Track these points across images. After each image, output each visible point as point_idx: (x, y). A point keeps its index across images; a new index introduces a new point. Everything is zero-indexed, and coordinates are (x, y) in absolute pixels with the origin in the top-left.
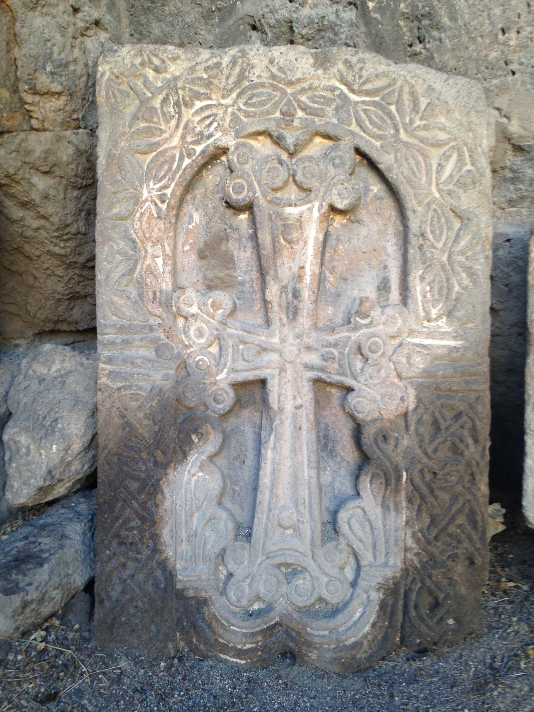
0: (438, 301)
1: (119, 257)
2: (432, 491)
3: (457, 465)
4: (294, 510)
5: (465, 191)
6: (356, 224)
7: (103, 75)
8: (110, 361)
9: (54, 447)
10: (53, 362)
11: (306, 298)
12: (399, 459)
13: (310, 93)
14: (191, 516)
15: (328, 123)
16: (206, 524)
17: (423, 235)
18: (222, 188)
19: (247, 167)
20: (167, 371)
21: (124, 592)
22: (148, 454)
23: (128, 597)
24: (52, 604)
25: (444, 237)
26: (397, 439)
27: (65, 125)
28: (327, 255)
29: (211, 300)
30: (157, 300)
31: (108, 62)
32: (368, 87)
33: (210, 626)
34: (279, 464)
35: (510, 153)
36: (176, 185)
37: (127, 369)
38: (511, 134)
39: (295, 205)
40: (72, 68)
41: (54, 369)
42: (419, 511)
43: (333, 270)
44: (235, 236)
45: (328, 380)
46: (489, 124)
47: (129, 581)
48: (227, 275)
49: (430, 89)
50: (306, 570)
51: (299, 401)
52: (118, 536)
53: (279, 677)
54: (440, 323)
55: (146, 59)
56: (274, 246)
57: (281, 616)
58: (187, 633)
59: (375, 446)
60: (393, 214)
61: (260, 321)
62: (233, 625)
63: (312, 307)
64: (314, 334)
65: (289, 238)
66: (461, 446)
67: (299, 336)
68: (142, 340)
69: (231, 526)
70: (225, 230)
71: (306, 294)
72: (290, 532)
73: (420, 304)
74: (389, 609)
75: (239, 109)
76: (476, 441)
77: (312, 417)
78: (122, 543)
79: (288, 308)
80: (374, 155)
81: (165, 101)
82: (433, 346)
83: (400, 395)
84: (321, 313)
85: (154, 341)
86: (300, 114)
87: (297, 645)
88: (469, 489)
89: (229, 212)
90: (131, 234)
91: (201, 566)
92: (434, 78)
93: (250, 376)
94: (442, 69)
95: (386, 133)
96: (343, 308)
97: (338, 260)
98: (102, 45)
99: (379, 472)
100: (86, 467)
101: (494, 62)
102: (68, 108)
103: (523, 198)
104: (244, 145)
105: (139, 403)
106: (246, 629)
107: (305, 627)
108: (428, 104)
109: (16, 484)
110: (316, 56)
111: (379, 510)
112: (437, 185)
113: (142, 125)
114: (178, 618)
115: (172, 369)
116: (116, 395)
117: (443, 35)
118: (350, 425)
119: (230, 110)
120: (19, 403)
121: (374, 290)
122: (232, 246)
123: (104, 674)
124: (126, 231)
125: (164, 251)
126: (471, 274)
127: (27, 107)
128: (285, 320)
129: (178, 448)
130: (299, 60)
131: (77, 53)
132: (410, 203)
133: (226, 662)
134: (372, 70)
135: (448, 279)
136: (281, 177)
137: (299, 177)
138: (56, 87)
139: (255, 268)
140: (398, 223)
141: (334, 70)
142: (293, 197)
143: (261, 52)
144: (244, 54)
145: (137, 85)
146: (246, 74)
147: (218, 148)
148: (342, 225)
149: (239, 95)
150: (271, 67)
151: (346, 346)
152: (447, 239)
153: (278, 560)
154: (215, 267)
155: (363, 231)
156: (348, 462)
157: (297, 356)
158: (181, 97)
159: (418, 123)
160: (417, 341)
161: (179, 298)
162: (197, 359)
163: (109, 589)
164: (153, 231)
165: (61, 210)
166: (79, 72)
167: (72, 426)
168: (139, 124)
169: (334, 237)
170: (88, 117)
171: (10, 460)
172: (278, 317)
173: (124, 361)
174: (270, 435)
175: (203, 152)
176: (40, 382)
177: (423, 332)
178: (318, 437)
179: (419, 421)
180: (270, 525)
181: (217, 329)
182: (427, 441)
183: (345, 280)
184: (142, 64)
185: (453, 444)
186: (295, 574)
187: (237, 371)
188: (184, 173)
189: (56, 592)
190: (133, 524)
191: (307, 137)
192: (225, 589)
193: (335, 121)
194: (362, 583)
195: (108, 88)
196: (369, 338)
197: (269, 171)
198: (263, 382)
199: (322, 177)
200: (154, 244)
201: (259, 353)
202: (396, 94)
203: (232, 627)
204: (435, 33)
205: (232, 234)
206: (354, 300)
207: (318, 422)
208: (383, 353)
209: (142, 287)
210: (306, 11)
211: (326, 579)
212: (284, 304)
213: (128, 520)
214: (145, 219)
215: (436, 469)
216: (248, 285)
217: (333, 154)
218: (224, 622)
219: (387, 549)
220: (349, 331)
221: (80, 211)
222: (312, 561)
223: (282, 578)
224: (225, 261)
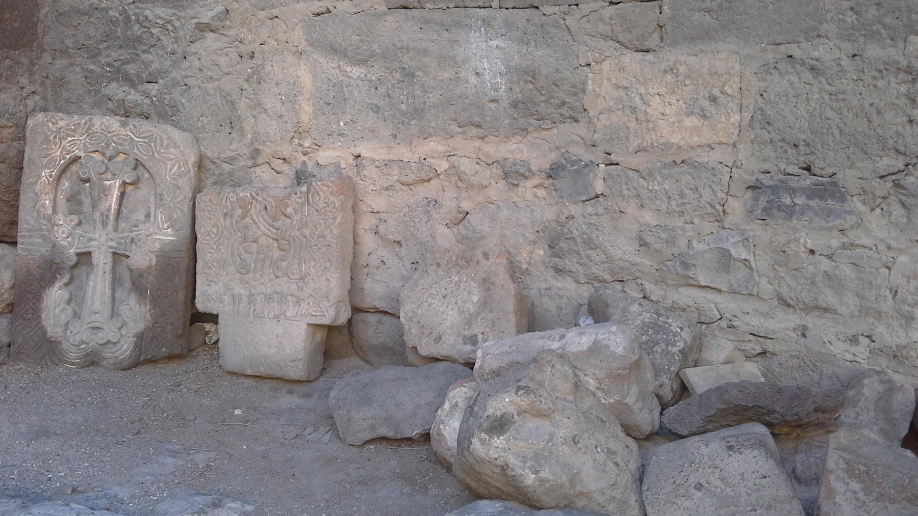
14: (55, 308)
18: (77, 172)
27: (13, 140)
43: (126, 208)
80: (143, 162)
81: (55, 137)
85: (43, 235)
89: (81, 183)
92: (176, 134)
93: (84, 250)
110: (121, 122)
122: (82, 196)
126: (182, 211)
131: (21, 107)
137: (111, 169)
138: (9, 124)
144: (90, 119)
153: (91, 325)
173: (29, 244)
179: (156, 270)
198: (90, 253)
213: (27, 310)
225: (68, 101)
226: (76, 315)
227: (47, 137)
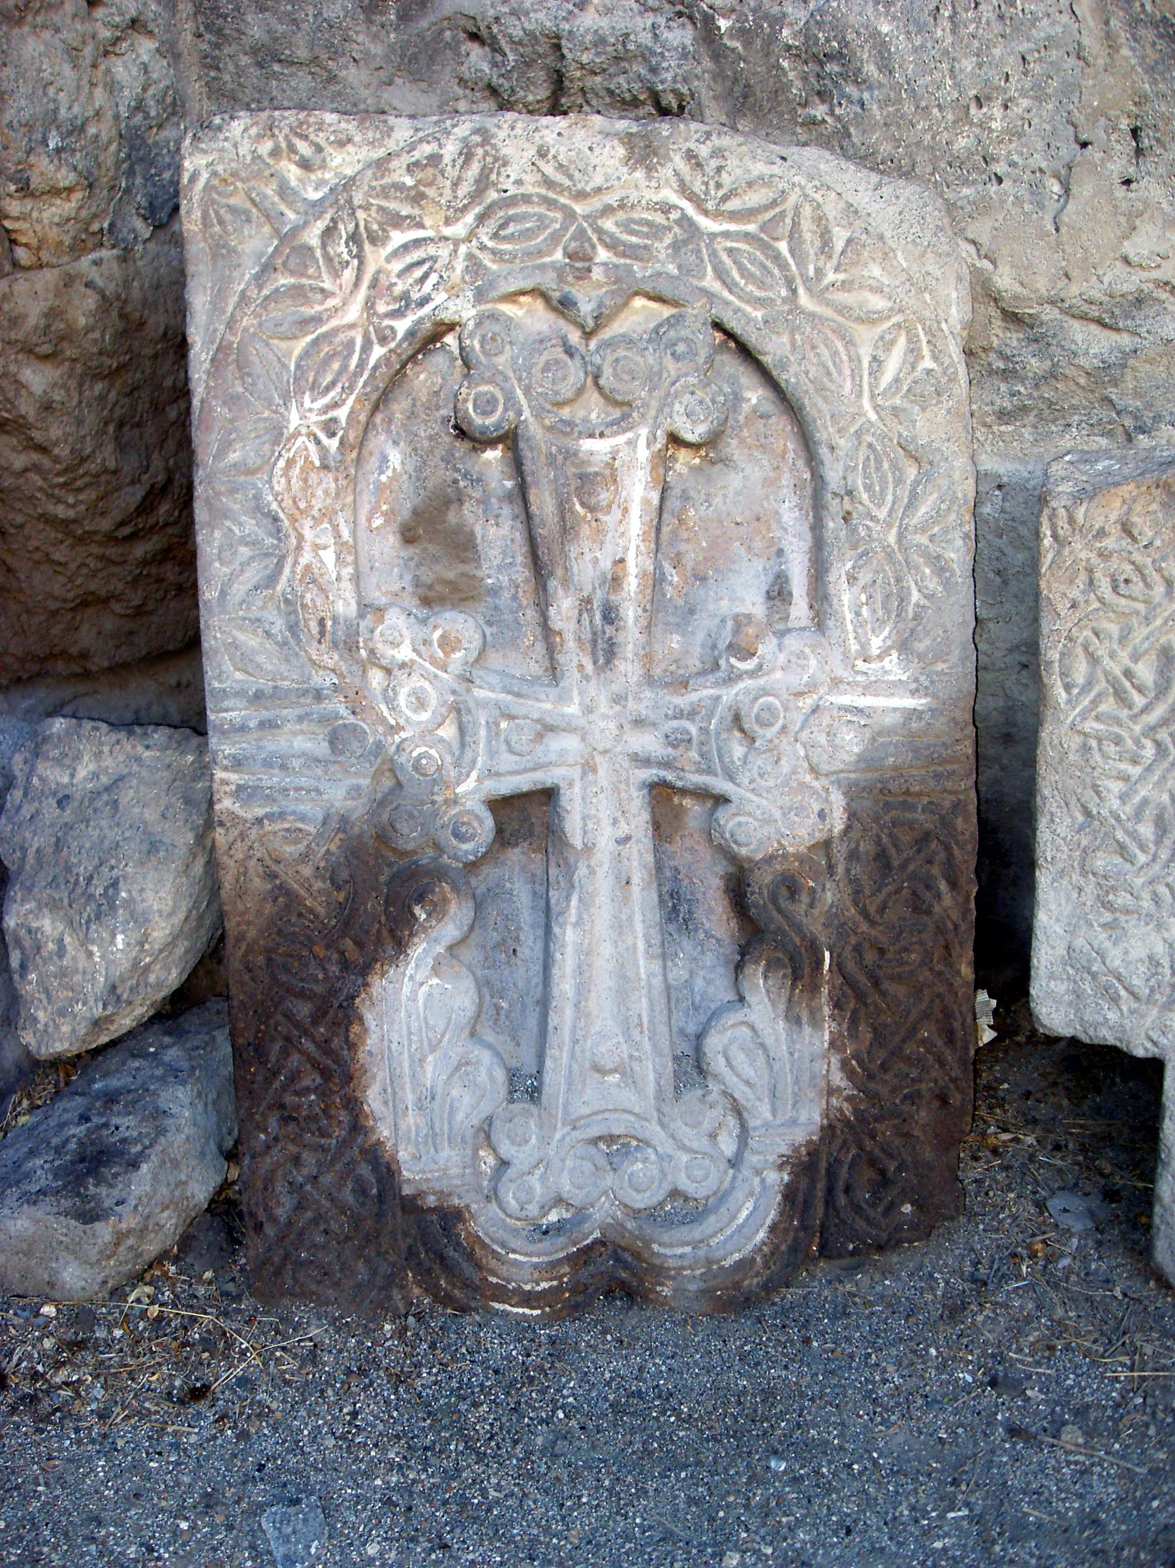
0: (881, 622)
1: (245, 551)
2: (876, 983)
3: (920, 932)
4: (622, 1040)
5: (924, 409)
6: (719, 466)
7: (193, 178)
8: (237, 764)
9: (120, 938)
10: (78, 758)
11: (631, 622)
12: (815, 926)
13: (621, 215)
14: (422, 1061)
15: (659, 274)
16: (451, 1076)
17: (850, 493)
19: (501, 361)
20: (355, 781)
21: (299, 1207)
22: (328, 947)
23: (309, 1214)
24: (160, 1236)
25: (889, 498)
26: (812, 891)
27: (78, 248)
28: (665, 530)
29: (439, 632)
30: (328, 637)
31: (205, 152)
32: (733, 204)
33: (470, 1256)
34: (588, 954)
35: (998, 323)
36: (357, 400)
37: (274, 779)
38: (999, 292)
39: (602, 435)
40: (92, 130)
41: (82, 773)
42: (854, 1021)
44: (477, 494)
45: (679, 784)
46: (960, 279)
47: (308, 1187)
48: (463, 574)
49: (851, 211)
50: (648, 1144)
51: (623, 829)
52: (282, 1107)
53: (605, 1332)
54: (886, 662)
55: (284, 145)
56: (563, 519)
57: (604, 1228)
58: (429, 1271)
59: (771, 907)
60: (790, 446)
61: (536, 669)
62: (514, 1251)
63: (642, 639)
64: (648, 694)
65: (593, 501)
66: (928, 895)
67: (618, 699)
68: (300, 719)
69: (500, 1076)
70: (455, 482)
71: (630, 613)
72: (614, 1078)
73: (850, 627)
74: (800, 1198)
75: (483, 247)
76: (953, 884)
77: (650, 858)
78: (286, 1120)
79: (594, 643)
80: (752, 338)
81: (329, 233)
82: (875, 710)
83: (816, 807)
84: (657, 647)
85: (324, 720)
86: (603, 255)
87: (635, 1275)
88: (940, 973)
89: (462, 447)
90: (269, 504)
91: (446, 1153)
92: (853, 184)
93: (523, 783)
94: (866, 159)
95: (771, 295)
96: (700, 637)
97: (688, 541)
98: (145, 68)
99: (780, 955)
100: (174, 973)
101: (963, 156)
102: (84, 213)
103: (1025, 409)
104: (493, 317)
105: (301, 847)
106: (539, 1256)
107: (647, 1244)
108: (849, 241)
109: (41, 1015)
110: (628, 139)
111: (781, 1024)
112: (873, 396)
113: (284, 280)
114: (410, 1247)
115: (364, 777)
116: (254, 833)
117: (866, 96)
118: (722, 868)
119: (463, 249)
120: (24, 850)
121: (760, 599)
122: (469, 514)
123: (284, 1349)
124: (258, 497)
125: (338, 536)
126: (941, 568)
127: (8, 224)
128: (589, 668)
129: (385, 933)
130: (597, 151)
132: (825, 431)
133: (506, 1314)
134: (739, 172)
135: (898, 580)
136: (571, 379)
138: (65, 177)
139: (520, 559)
140: (801, 463)
141: (666, 172)
142: (593, 416)
143: (518, 131)
145: (265, 197)
146: (493, 177)
147: (441, 323)
148: (692, 468)
149: (481, 219)
150: (541, 163)
151: (710, 716)
152: (894, 503)
153: (595, 1132)
154: (436, 560)
155: (734, 481)
156: (718, 941)
157: (618, 738)
158: (362, 224)
159: (831, 277)
160: (845, 700)
161: (372, 632)
162: (414, 754)
163: (272, 1204)
164: (313, 495)
165: (74, 429)
166: (104, 137)
167: (149, 894)
168: (276, 280)
169: (677, 492)
170: (119, 224)
171: (23, 966)
172: (575, 663)
173: (268, 764)
174: (568, 898)
175: (411, 334)
176: (59, 803)
177: (857, 684)
178: (660, 896)
179: (853, 855)
180: (575, 1067)
181: (454, 692)
182: (867, 892)
183: (703, 579)
184: (275, 153)
185: (914, 893)
186: (627, 1154)
187: (498, 774)
188: (372, 376)
189: (166, 1214)
190: (306, 1082)
191: (619, 301)
192: (495, 1190)
193: (672, 269)
194: (754, 1160)
195: (207, 203)
196: (756, 699)
197: (546, 369)
198: (548, 795)
199: (652, 379)
200: (317, 521)
201: (540, 736)
202: (788, 221)
203: (511, 1256)
204: (850, 89)
205: (469, 490)
206: (723, 621)
207: (659, 867)
208: (784, 727)
209: (295, 612)
210: (589, 21)
211: (685, 1158)
212: (587, 635)
214: (296, 471)
215: (884, 940)
216: (506, 595)
217: (672, 333)
218: (495, 1247)
219: (795, 1095)
220: (717, 684)
221: (106, 424)
222: (658, 1128)
223: (602, 1162)
224: (457, 546)
225: (268, 56)
226: (526, 1087)
227: (288, 238)
